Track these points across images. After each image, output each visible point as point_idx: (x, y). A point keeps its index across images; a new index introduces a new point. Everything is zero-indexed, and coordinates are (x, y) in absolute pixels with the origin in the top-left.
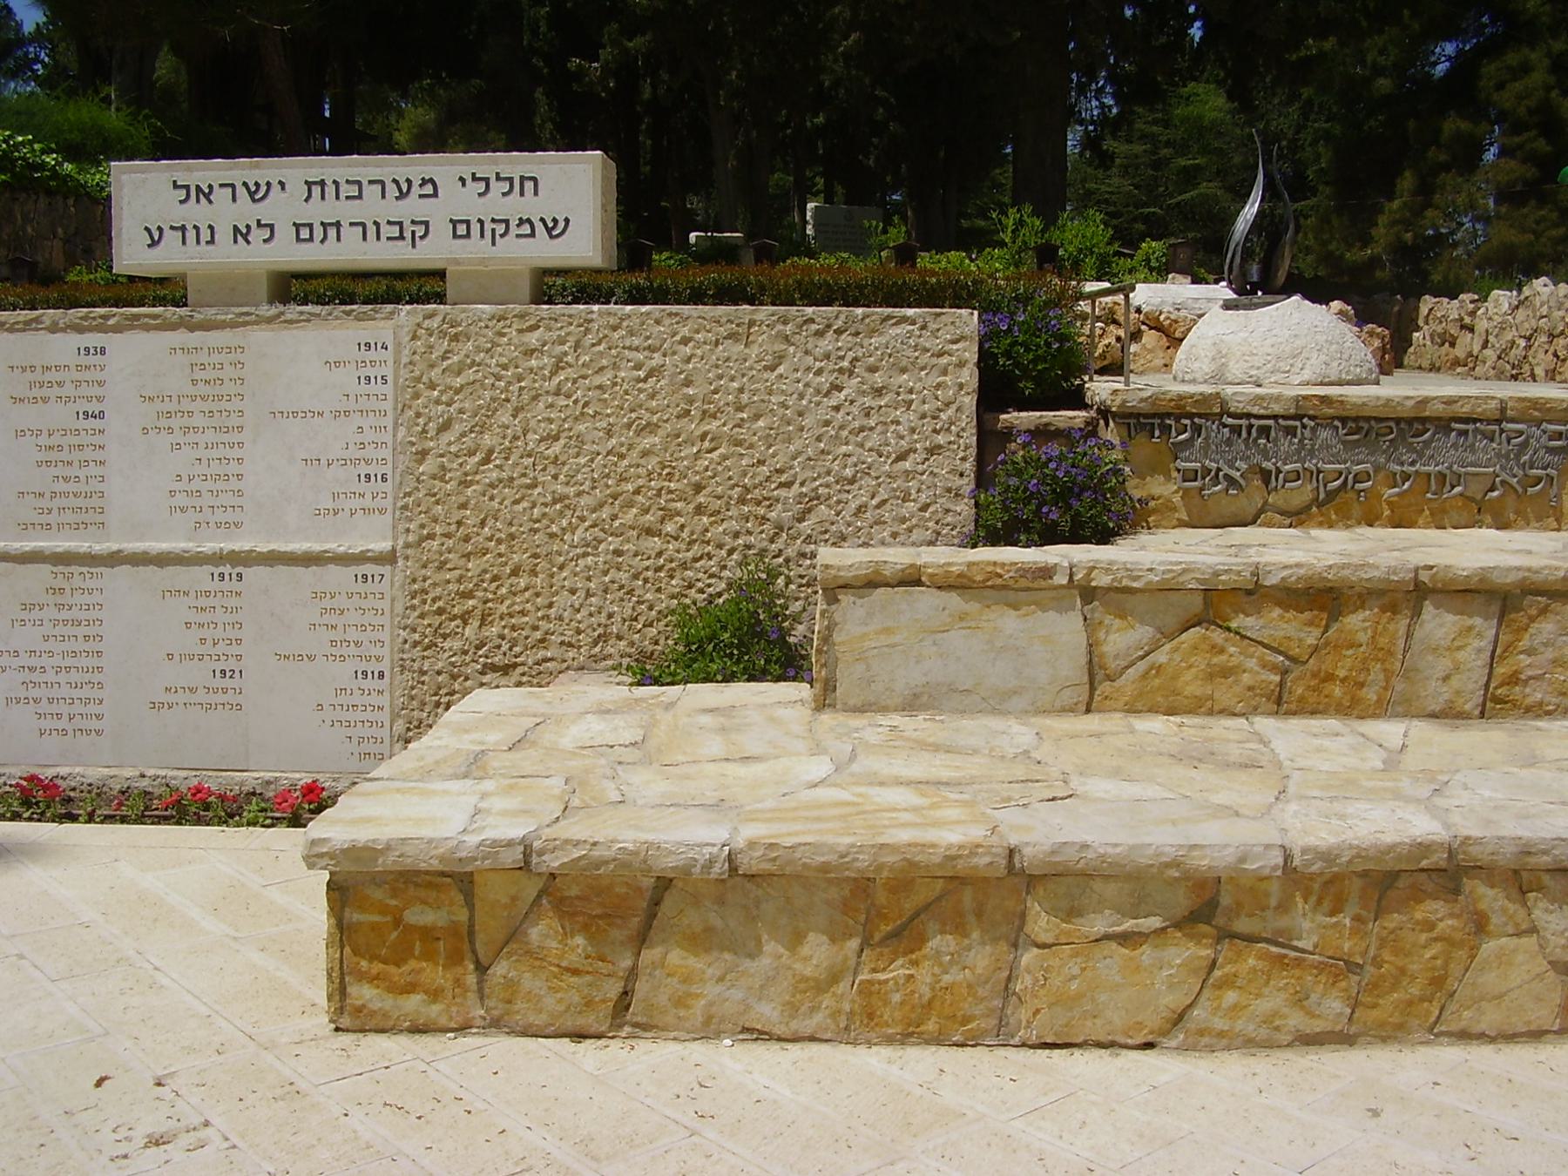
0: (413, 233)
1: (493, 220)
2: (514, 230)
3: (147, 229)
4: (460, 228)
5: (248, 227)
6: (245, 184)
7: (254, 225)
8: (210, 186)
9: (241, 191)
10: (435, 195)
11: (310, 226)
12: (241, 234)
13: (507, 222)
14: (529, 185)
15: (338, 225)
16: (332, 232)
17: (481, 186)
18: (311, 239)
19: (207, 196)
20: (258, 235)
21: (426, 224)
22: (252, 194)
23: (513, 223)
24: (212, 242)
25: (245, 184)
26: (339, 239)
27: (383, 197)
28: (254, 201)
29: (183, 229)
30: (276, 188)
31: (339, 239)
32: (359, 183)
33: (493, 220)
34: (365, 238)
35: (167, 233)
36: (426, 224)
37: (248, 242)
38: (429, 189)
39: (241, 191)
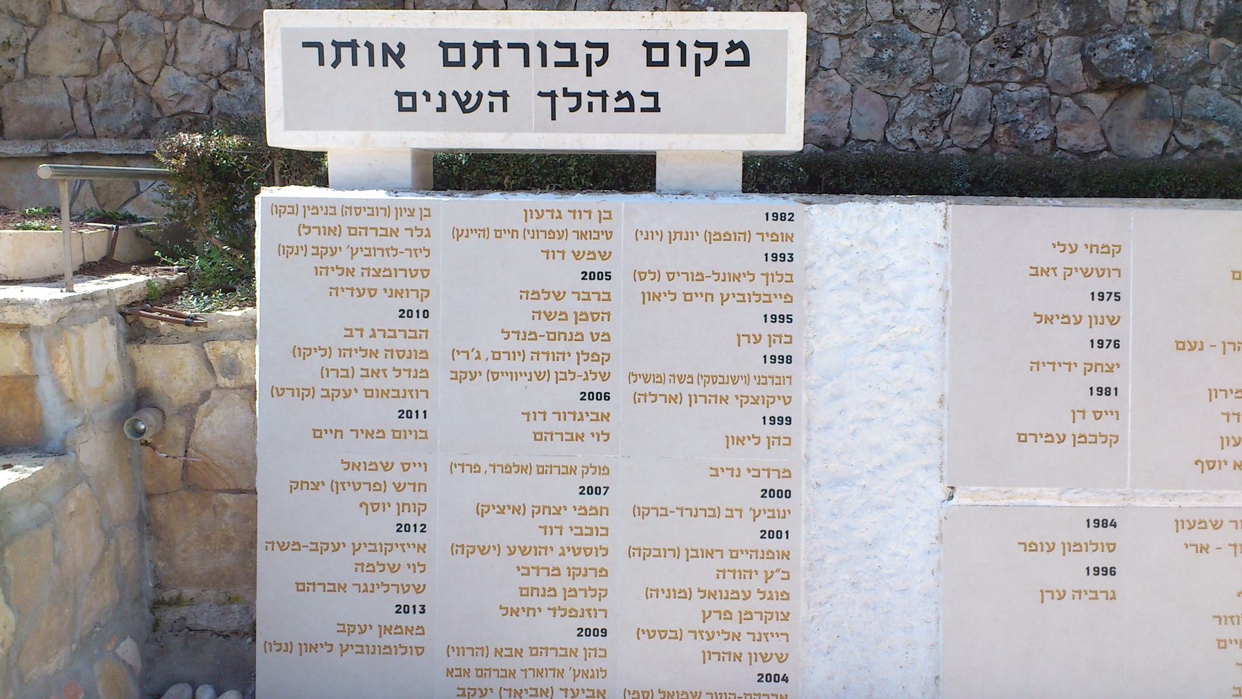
0: (589, 57)
2: (723, 56)
6: (455, 94)
11: (461, 46)
13: (714, 46)
15: (495, 46)
16: (488, 54)
18: (461, 63)
21: (605, 46)
22: (462, 105)
25: (455, 94)
26: (496, 64)
28: (465, 111)
31: (496, 64)
33: (698, 44)
34: (527, 64)
36: (605, 46)
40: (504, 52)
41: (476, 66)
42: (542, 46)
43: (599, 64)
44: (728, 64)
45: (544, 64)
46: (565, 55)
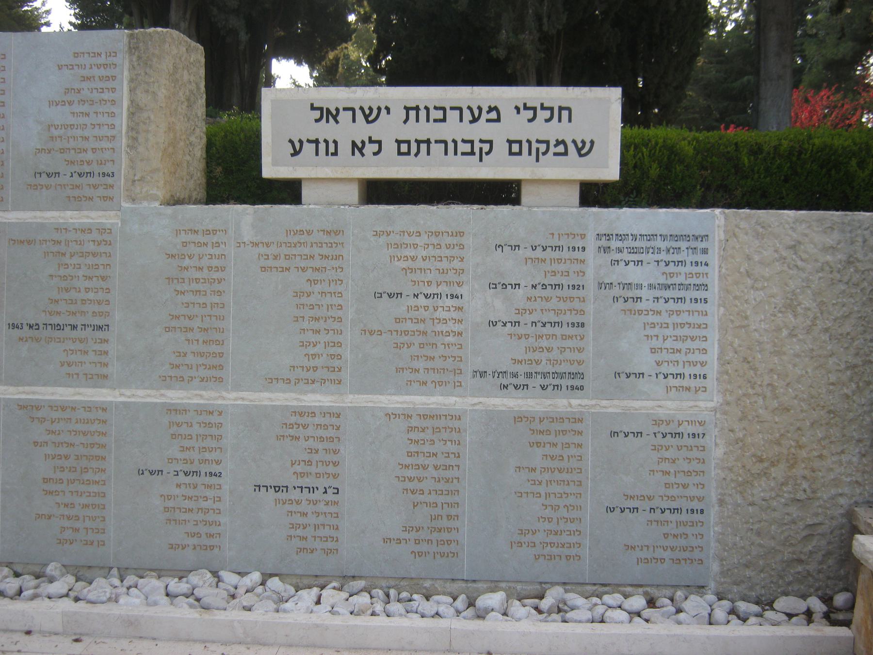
0: (481, 149)
1: (538, 141)
2: (552, 149)
3: (291, 141)
4: (515, 147)
5: (363, 142)
7: (367, 142)
8: (337, 110)
9: (359, 113)
10: (498, 120)
12: (357, 148)
14: (565, 114)
15: (428, 142)
16: (424, 147)
17: (530, 114)
18: (408, 153)
19: (335, 118)
20: (370, 148)
21: (491, 142)
23: (552, 143)
24: (335, 154)
26: (428, 153)
27: (461, 120)
29: (317, 142)
30: (384, 111)
31: (428, 153)
32: (444, 109)
33: (538, 141)
34: (446, 153)
35: (305, 144)
36: (491, 142)
37: (363, 155)
38: (493, 115)
39: (359, 113)
40: (433, 146)
41: (416, 155)
42: (455, 142)
43: (487, 153)
44: (555, 154)
45: (456, 153)
46: (467, 148)
